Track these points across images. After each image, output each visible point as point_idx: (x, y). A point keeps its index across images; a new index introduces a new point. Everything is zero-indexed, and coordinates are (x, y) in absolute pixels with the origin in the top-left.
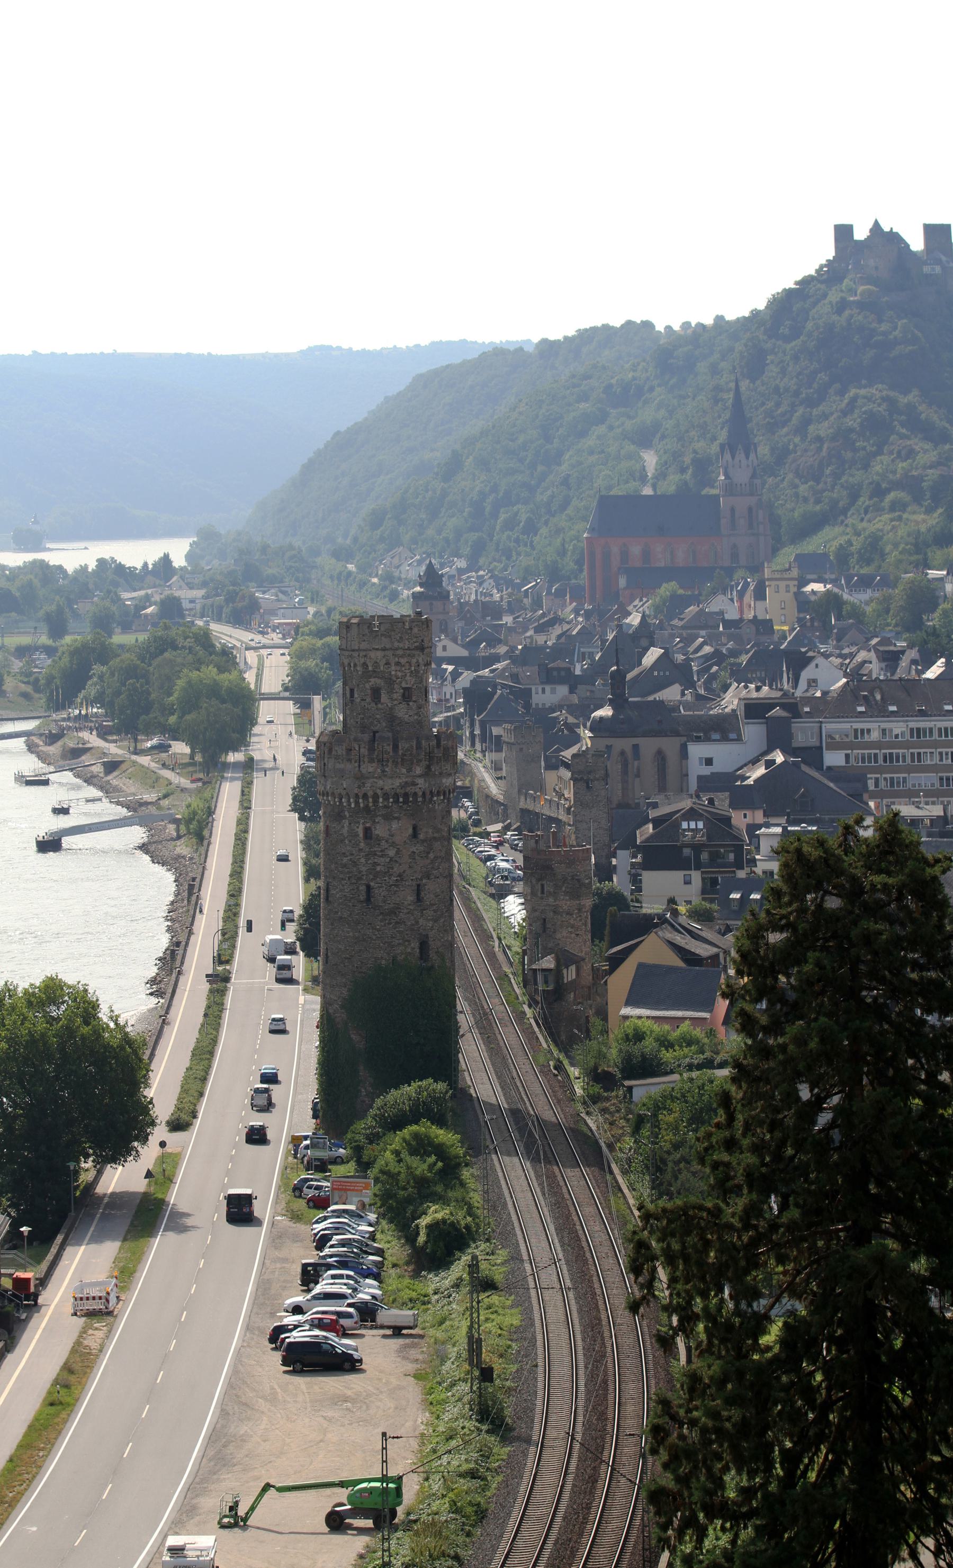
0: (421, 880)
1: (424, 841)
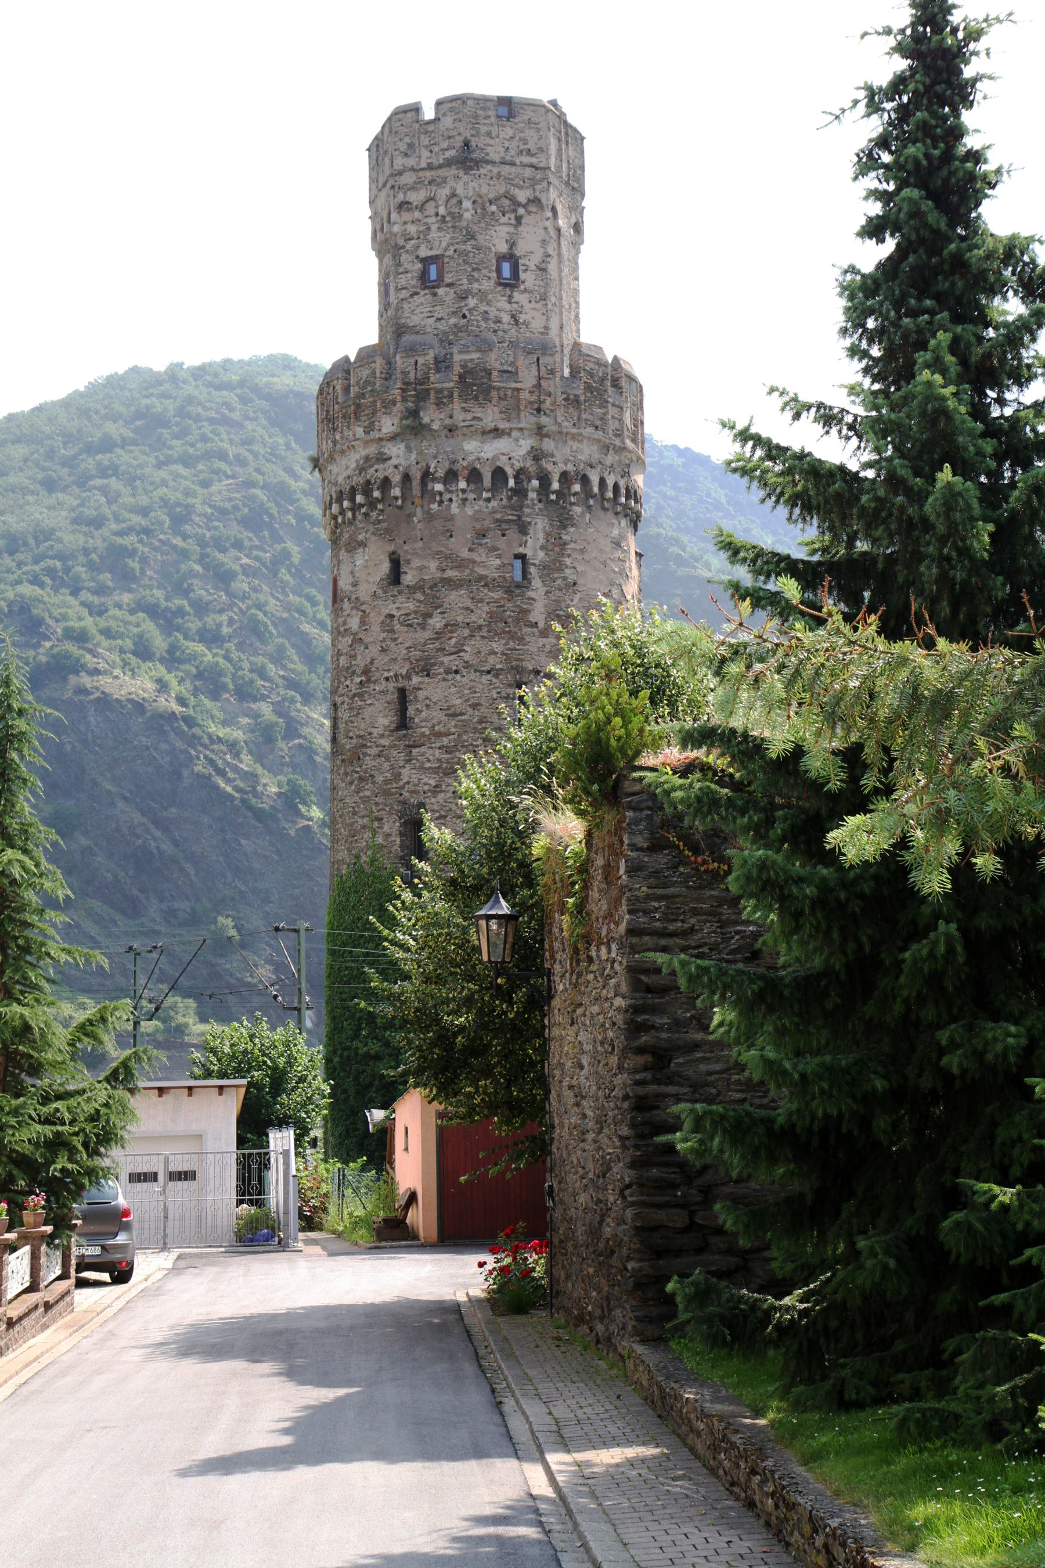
0: (408, 677)
1: (413, 589)
